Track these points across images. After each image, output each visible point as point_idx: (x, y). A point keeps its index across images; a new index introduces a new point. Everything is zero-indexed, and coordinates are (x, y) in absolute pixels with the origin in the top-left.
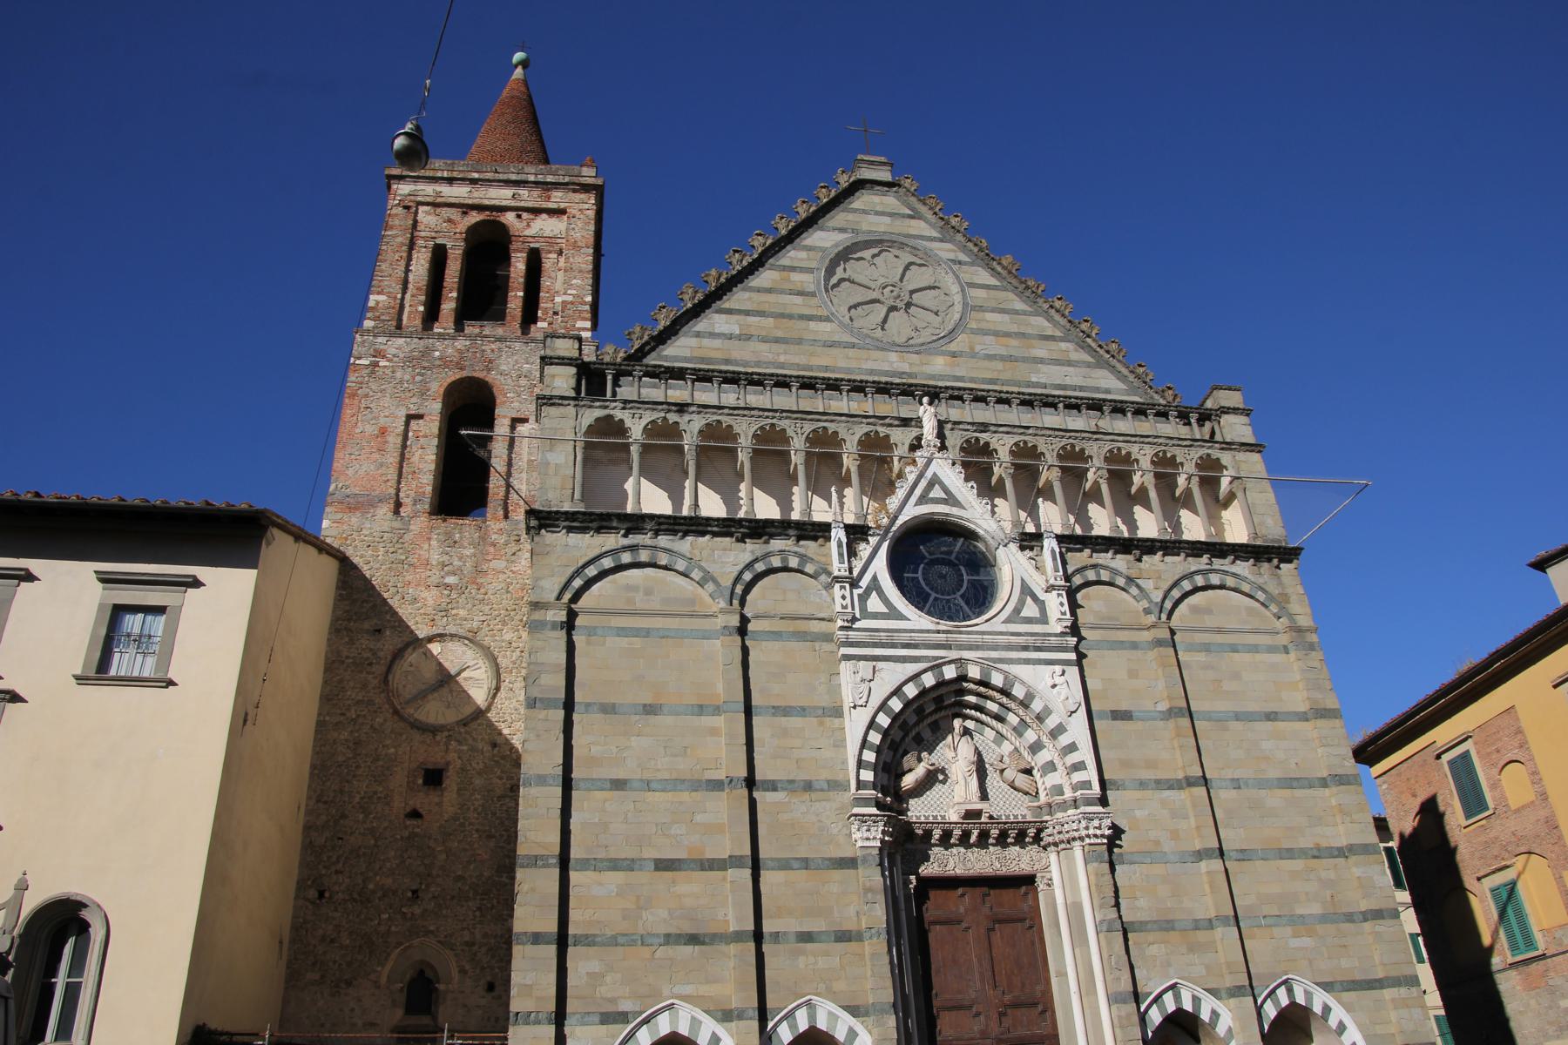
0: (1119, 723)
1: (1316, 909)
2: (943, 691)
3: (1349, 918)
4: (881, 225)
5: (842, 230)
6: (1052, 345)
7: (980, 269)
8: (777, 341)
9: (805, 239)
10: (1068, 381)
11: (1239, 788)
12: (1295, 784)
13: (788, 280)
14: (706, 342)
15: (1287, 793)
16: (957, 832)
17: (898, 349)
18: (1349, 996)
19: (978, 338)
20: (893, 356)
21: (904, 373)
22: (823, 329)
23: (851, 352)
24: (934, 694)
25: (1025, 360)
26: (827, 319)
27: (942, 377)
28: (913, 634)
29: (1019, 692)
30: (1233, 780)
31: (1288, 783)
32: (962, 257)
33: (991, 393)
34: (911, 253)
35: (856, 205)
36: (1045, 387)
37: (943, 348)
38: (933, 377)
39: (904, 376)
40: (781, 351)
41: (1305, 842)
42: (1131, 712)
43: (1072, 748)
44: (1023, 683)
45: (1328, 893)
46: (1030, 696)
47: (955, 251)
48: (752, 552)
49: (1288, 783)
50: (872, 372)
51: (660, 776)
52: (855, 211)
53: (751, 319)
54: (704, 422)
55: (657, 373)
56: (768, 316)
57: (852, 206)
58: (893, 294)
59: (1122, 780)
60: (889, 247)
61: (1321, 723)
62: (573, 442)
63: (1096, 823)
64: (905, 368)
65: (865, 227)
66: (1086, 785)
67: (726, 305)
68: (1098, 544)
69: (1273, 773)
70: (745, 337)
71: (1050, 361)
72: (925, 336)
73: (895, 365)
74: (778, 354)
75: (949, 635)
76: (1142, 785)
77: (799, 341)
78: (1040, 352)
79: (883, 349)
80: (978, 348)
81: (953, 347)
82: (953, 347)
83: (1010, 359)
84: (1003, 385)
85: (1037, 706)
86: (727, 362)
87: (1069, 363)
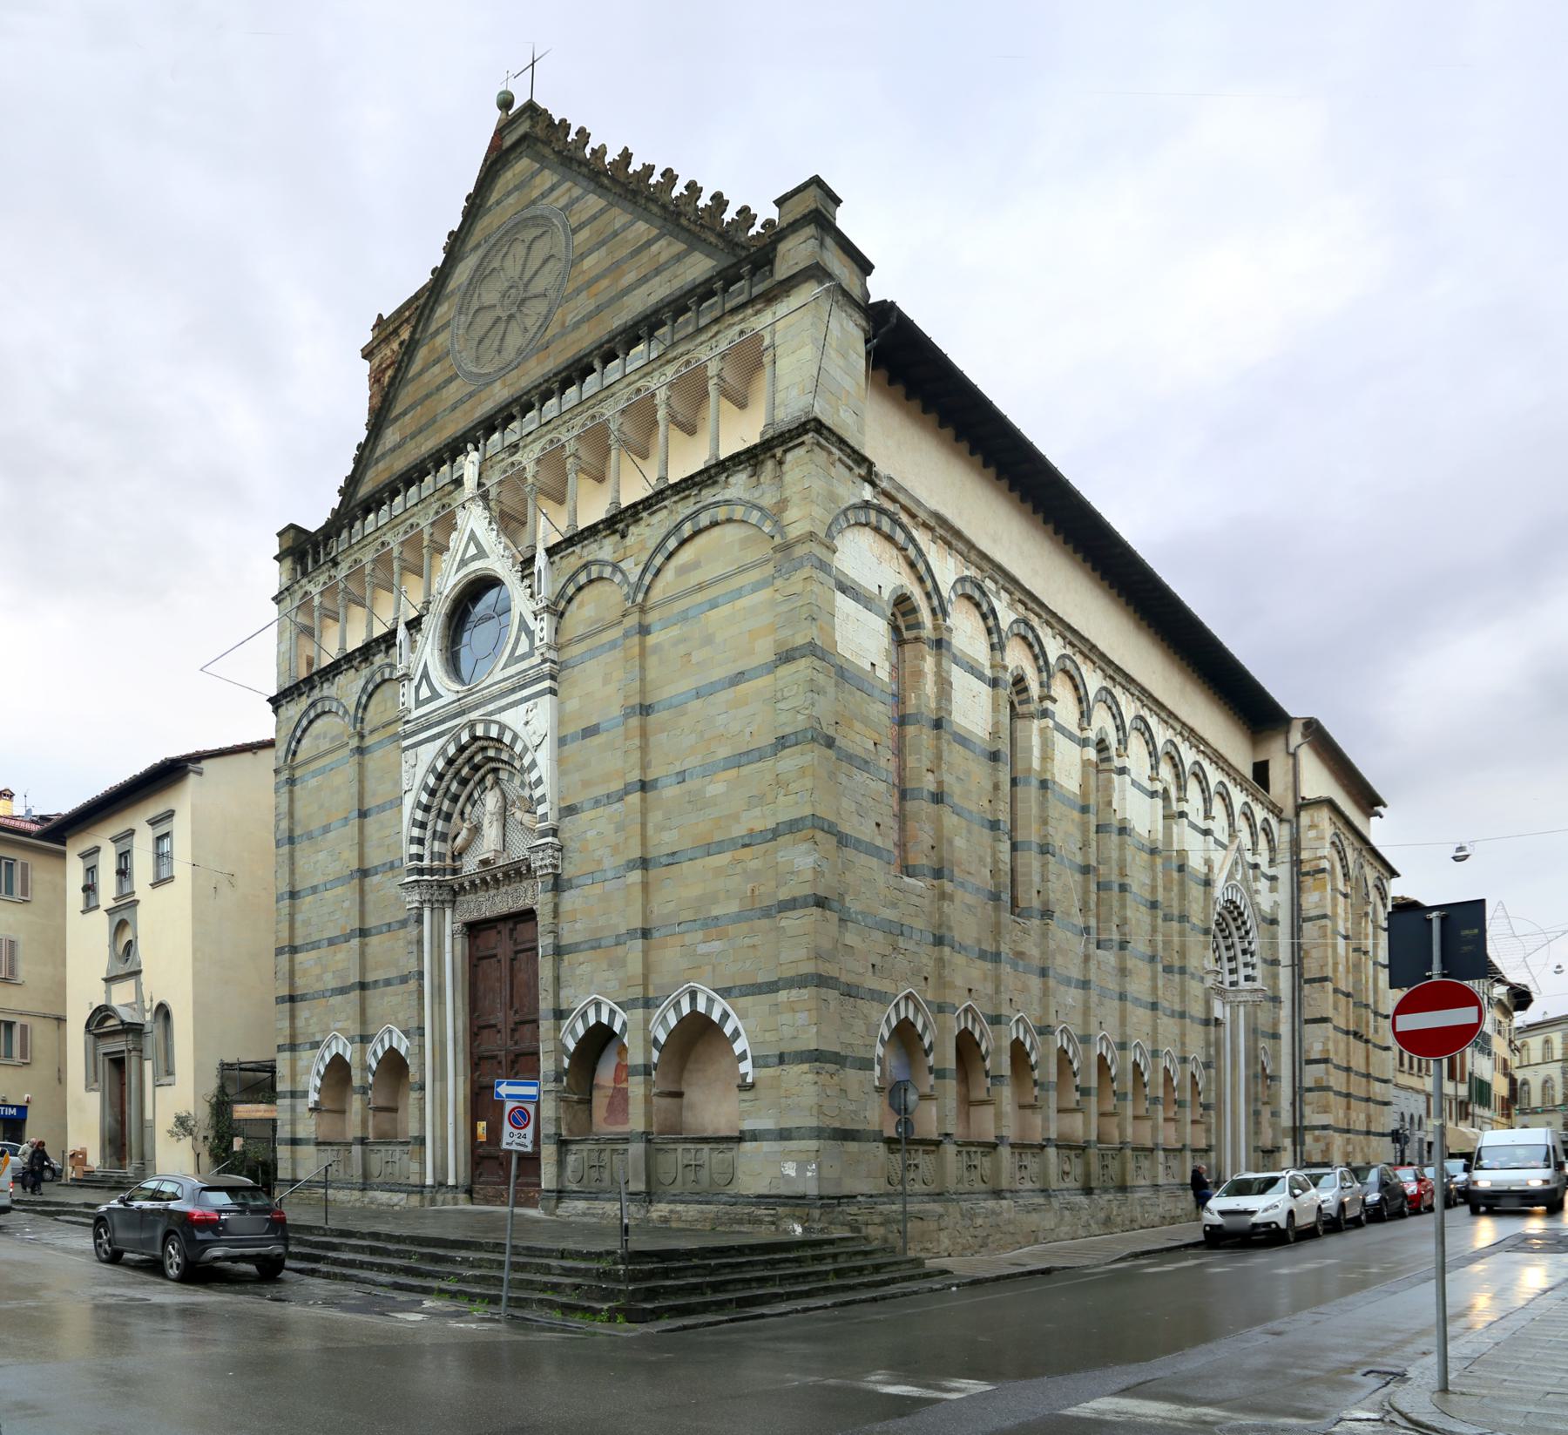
1: (733, 907)
2: (467, 754)
3: (767, 913)
11: (684, 781)
12: (744, 760)
15: (734, 772)
16: (478, 881)
18: (747, 1001)
30: (678, 773)
31: (738, 760)
33: (533, 393)
41: (739, 830)
45: (750, 886)
46: (515, 737)
49: (738, 760)
51: (331, 878)
61: (785, 670)
68: (585, 539)
69: (723, 752)
82: (549, 333)
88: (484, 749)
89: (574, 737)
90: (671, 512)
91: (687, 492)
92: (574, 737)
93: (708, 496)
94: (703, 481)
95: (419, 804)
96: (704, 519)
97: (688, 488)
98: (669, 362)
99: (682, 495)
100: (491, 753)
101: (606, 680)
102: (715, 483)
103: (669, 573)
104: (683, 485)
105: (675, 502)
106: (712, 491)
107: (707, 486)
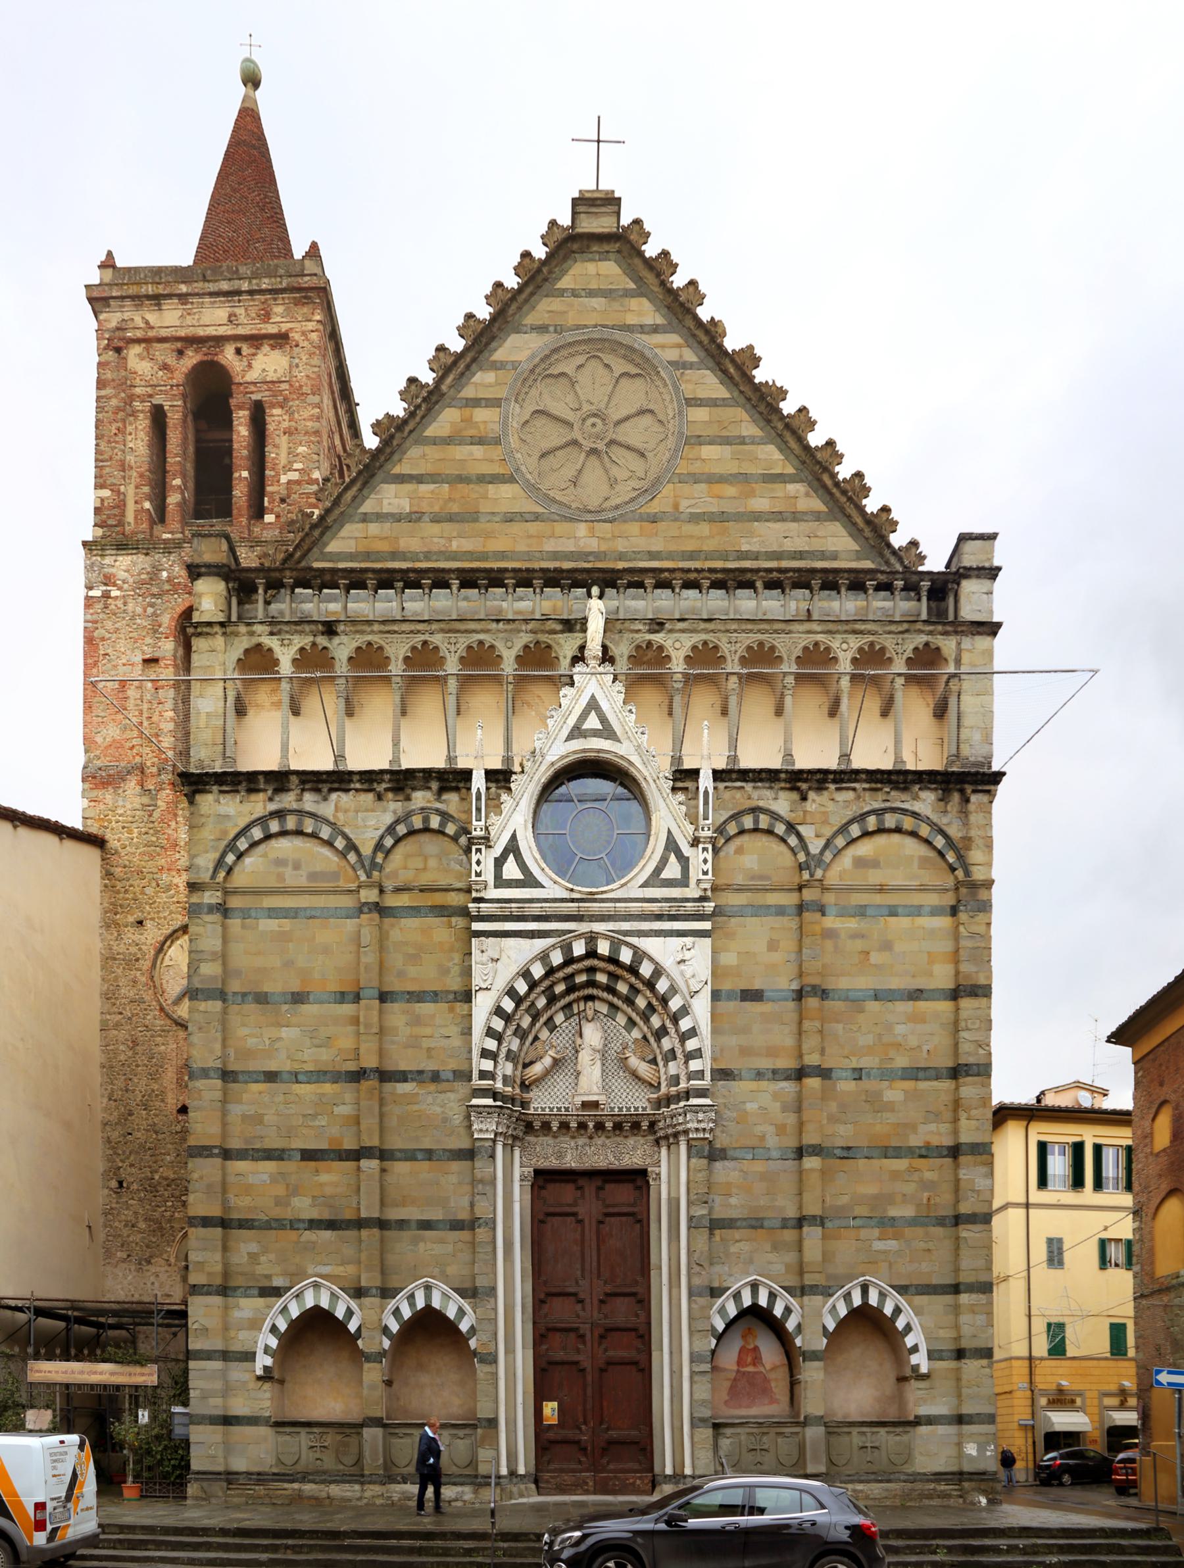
0: (747, 1004)
4: (594, 311)
5: (542, 329)
6: (780, 490)
7: (708, 372)
8: (451, 518)
9: (496, 350)
10: (789, 546)
13: (468, 421)
14: (374, 528)
17: (589, 517)
19: (686, 489)
20: (582, 529)
21: (591, 553)
22: (506, 496)
23: (533, 528)
24: (560, 975)
25: (740, 517)
26: (510, 479)
27: (637, 555)
28: (544, 905)
29: (646, 970)
32: (690, 356)
34: (624, 357)
35: (565, 283)
36: (756, 559)
37: (642, 510)
38: (621, 557)
39: (591, 558)
40: (455, 534)
42: (762, 991)
43: (693, 1032)
44: (651, 959)
47: (679, 346)
48: (395, 812)
50: (555, 556)
52: (562, 293)
53: (424, 488)
54: (355, 645)
55: (323, 581)
56: (443, 482)
57: (561, 284)
58: (594, 430)
59: (740, 1070)
60: (598, 350)
62: (221, 684)
63: (701, 1116)
64: (593, 545)
65: (572, 319)
66: (700, 1074)
67: (397, 470)
70: (414, 517)
71: (772, 516)
72: (624, 493)
73: (581, 543)
74: (450, 539)
75: (581, 904)
76: (759, 1075)
77: (473, 517)
78: (760, 504)
79: (571, 520)
80: (684, 504)
81: (655, 507)
83: (721, 518)
84: (706, 559)
85: (662, 986)
86: (394, 555)
87: (796, 517)
88: (592, 970)
89: (730, 995)
90: (859, 797)
91: (879, 786)
92: (730, 995)
93: (898, 799)
94: (898, 782)
95: (499, 1011)
96: (890, 821)
97: (881, 782)
98: (855, 632)
99: (874, 785)
100: (602, 978)
101: (773, 946)
102: (905, 789)
103: (846, 860)
104: (879, 776)
105: (864, 789)
106: (904, 796)
107: (897, 789)
